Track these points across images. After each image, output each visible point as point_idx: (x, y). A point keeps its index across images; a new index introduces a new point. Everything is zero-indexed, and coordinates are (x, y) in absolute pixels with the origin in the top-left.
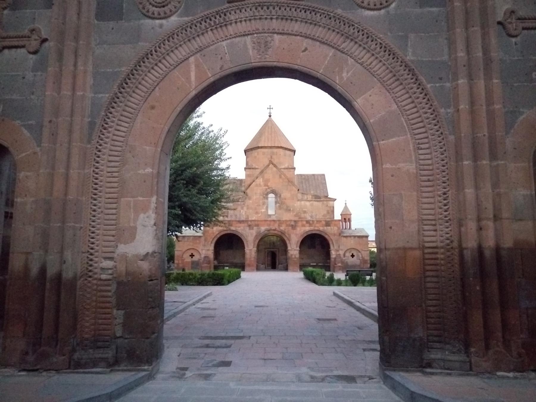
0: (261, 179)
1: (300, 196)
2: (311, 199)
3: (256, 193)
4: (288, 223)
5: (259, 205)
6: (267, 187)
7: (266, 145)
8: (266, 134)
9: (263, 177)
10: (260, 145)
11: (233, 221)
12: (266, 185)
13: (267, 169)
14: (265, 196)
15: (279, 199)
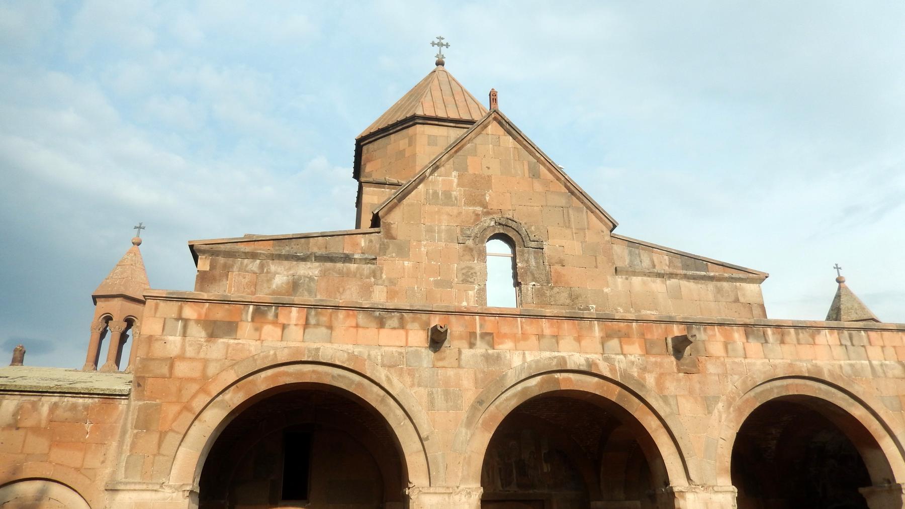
0: (455, 173)
1: (621, 253)
2: (667, 270)
3: (430, 230)
4: (657, 332)
5: (448, 284)
6: (479, 209)
7: (441, 114)
8: (437, 94)
9: (462, 169)
10: (420, 112)
11: (337, 308)
12: (475, 199)
13: (478, 140)
14: (470, 243)
15: (533, 262)
